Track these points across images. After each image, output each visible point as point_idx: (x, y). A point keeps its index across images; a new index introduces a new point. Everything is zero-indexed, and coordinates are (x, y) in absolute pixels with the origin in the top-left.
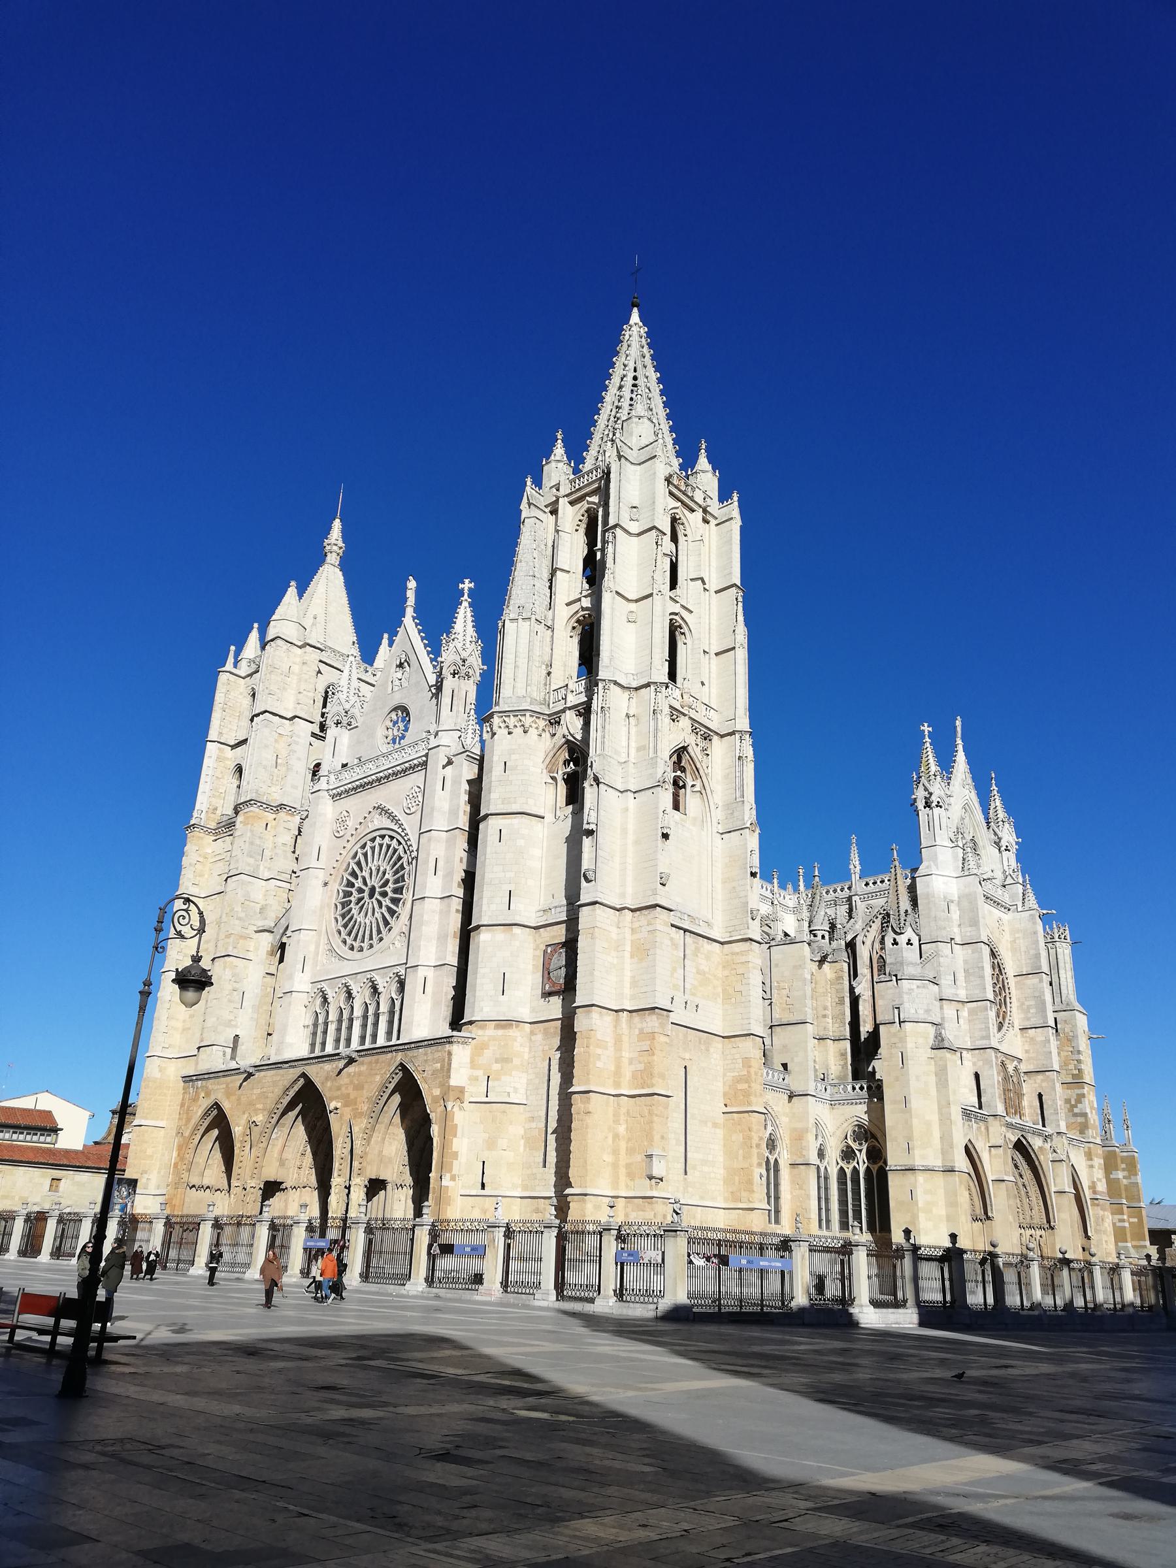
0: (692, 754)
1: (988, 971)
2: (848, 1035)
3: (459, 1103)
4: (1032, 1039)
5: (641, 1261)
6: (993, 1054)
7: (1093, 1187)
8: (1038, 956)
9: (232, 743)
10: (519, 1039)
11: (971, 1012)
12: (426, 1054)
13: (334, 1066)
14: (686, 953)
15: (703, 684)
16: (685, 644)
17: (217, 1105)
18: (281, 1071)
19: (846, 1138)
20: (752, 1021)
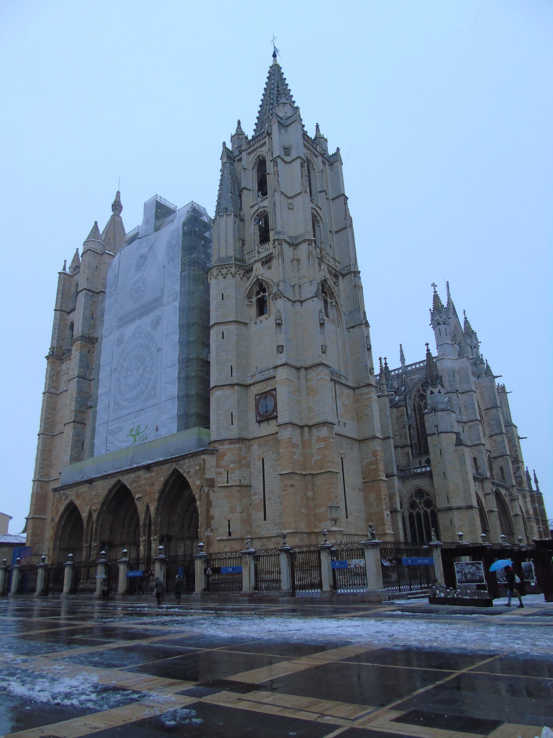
0: (329, 284)
1: (476, 406)
2: (409, 443)
3: (211, 488)
4: (495, 440)
5: (349, 567)
6: (483, 448)
7: (527, 512)
8: (495, 399)
9: (69, 310)
10: (244, 449)
11: (470, 427)
12: (189, 462)
13: (137, 474)
14: (337, 393)
15: (331, 248)
16: (319, 226)
17: (71, 504)
18: (107, 480)
19: (412, 497)
20: (376, 430)
